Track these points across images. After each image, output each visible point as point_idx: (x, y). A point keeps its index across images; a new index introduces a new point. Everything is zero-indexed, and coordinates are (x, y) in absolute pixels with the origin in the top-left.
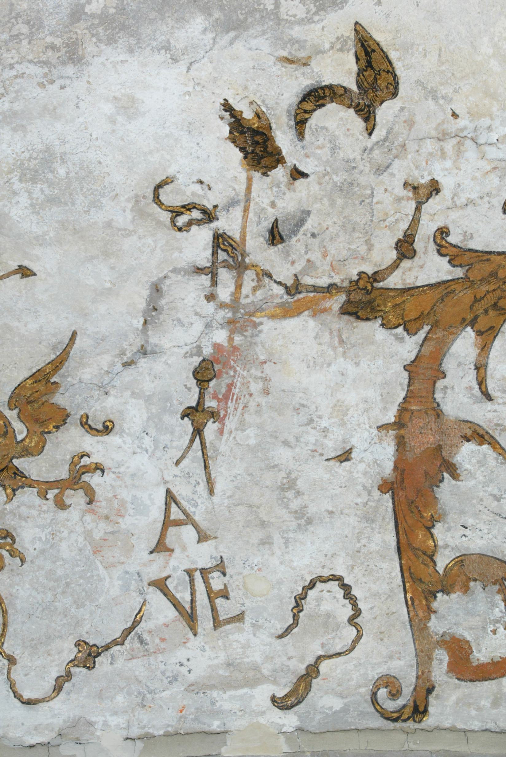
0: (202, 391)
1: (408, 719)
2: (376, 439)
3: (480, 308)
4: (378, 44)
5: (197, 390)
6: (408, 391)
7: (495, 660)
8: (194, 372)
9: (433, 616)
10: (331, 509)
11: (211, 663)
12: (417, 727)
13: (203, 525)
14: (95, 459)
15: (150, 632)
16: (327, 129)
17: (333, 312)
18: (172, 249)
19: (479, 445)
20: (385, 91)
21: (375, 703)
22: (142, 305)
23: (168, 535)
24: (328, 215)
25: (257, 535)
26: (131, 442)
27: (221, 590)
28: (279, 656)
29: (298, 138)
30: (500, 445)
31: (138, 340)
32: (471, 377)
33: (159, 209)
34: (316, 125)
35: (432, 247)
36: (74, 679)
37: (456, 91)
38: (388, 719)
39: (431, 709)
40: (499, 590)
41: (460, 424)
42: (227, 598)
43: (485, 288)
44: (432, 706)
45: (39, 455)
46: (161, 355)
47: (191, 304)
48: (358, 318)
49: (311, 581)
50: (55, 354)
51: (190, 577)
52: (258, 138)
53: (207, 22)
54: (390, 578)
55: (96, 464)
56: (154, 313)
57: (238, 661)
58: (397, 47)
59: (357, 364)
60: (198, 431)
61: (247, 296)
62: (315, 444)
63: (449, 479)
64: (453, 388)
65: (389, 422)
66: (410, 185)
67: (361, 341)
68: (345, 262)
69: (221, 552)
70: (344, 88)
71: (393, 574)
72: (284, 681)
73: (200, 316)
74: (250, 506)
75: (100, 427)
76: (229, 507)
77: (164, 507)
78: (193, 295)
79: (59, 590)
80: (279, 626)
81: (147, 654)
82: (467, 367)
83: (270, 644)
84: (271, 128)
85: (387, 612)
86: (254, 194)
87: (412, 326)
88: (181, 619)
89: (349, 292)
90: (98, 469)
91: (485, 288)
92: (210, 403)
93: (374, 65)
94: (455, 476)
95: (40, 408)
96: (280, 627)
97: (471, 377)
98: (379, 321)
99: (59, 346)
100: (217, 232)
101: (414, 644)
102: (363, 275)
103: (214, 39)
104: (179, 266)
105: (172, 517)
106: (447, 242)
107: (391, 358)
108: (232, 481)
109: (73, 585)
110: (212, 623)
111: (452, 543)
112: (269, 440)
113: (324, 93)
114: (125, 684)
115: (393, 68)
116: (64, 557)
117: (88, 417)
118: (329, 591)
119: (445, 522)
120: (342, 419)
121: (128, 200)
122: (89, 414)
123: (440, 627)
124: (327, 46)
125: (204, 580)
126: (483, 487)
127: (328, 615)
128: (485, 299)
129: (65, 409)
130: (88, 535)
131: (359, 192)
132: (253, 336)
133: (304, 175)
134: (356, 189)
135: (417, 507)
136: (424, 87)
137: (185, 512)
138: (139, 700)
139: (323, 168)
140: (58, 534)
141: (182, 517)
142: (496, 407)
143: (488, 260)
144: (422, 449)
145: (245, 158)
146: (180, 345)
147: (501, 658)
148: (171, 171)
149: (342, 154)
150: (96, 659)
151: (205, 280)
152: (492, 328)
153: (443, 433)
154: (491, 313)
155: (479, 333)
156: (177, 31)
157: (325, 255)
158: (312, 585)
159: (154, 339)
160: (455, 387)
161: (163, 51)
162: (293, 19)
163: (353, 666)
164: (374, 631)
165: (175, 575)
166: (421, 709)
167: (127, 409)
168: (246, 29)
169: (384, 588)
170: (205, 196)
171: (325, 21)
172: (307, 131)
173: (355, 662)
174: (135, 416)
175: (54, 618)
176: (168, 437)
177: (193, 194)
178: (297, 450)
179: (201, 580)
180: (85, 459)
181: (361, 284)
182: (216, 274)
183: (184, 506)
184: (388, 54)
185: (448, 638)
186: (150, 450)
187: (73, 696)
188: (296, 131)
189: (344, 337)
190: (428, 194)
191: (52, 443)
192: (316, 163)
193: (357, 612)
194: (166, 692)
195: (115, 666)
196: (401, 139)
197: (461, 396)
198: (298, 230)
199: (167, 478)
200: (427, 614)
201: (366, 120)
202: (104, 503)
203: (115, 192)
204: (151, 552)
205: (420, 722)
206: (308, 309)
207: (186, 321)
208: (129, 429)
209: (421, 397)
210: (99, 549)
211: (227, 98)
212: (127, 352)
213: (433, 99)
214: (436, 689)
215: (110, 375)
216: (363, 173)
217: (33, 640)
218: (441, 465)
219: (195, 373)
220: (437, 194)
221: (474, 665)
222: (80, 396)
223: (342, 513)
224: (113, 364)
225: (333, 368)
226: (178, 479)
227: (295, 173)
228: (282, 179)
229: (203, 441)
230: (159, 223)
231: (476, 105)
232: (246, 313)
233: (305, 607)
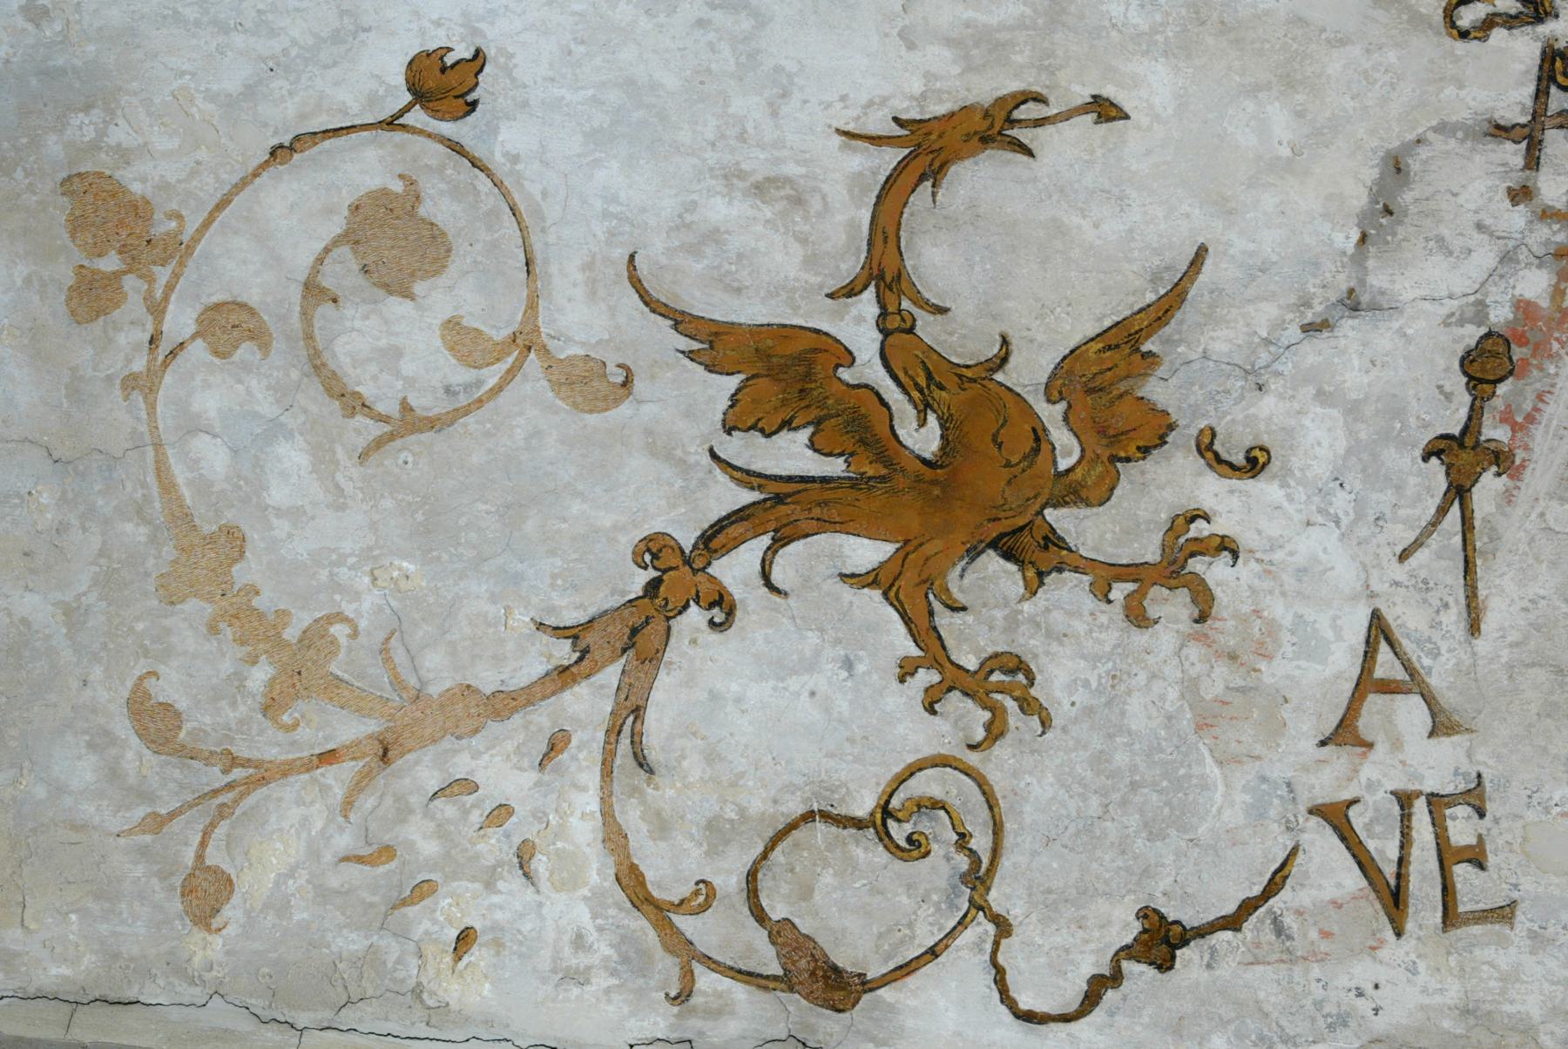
0: (1478, 403)
5: (1467, 399)
11: (1427, 1001)
13: (1448, 698)
14: (1221, 526)
15: (1299, 913)
18: (1441, 79)
22: (1358, 198)
23: (1364, 711)
26: (1304, 498)
31: (1341, 277)
42: (1481, 866)
45: (1101, 505)
46: (1391, 316)
47: (1472, 206)
50: (1157, 292)
51: (1402, 808)
55: (1223, 537)
56: (1383, 221)
57: (1487, 1007)
60: (1459, 491)
69: (1478, 763)
73: (1491, 234)
75: (1239, 459)
76: (1510, 667)
77: (1361, 648)
78: (1480, 186)
79: (1116, 796)
81: (1290, 958)
88: (1373, 896)
90: (1226, 549)
92: (1494, 432)
95: (1112, 403)
99: (1166, 276)
100: (1551, 46)
104: (1454, 119)
105: (1379, 673)
108: (1525, 610)
109: (1145, 791)
110: (1439, 914)
114: (1233, 1015)
116: (1134, 728)
117: (1214, 435)
122: (1217, 429)
125: (1433, 819)
130: (1190, 687)
140: (1125, 677)
141: (1400, 674)
146: (1436, 295)
150: (1178, 952)
151: (1513, 154)
159: (1378, 279)
165: (1369, 799)
167: (1302, 426)
174: (1319, 444)
175: (1099, 853)
176: (1388, 496)
179: (1427, 818)
180: (1200, 523)
182: (1540, 142)
183: (1408, 650)
186: (1345, 521)
187: (1121, 1021)
191: (1131, 482)
195: (1217, 973)
199: (1376, 586)
202: (1231, 623)
204: (1323, 743)
207: (1456, 244)
208: (1302, 470)
210: (1209, 721)
212: (1316, 302)
215: (1272, 349)
217: (1050, 891)
219: (1467, 361)
222: (1201, 388)
224: (1280, 325)
226: (1402, 590)
229: (1468, 514)
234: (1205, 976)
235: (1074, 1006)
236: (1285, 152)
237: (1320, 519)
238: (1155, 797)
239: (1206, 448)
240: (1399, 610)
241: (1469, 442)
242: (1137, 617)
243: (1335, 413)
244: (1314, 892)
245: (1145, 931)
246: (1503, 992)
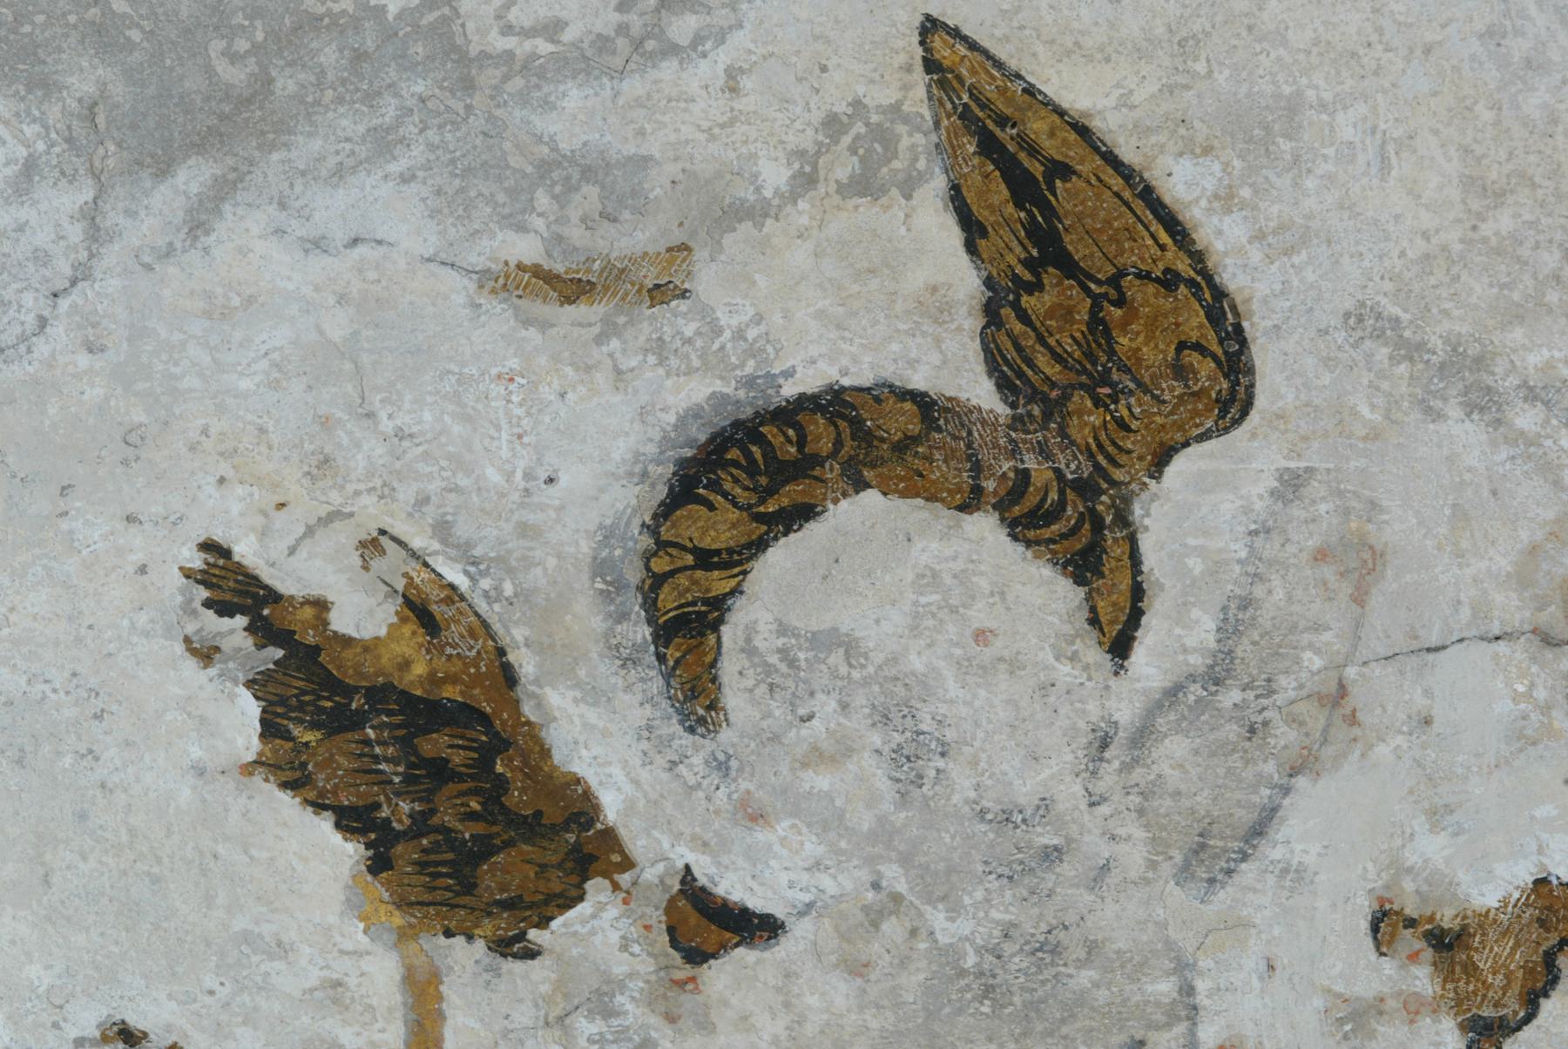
4: (1083, 131)
16: (850, 647)
20: (1171, 389)
29: (684, 717)
34: (783, 629)
52: (436, 744)
53: (30, 130)
58: (1201, 132)
66: (1411, 923)
84: (509, 676)
103: (91, 217)
113: (801, 443)
115: (1198, 257)
124: (775, 175)
131: (1102, 995)
134: (1086, 977)
136: (1401, 342)
139: (865, 875)
145: (379, 864)
149: (963, 784)
162: (544, 47)
171: (739, 39)
172: (729, 667)
184: (1155, 176)
188: (668, 677)
190: (1529, 971)
192: (812, 847)
211: (219, 536)
213: (1470, 408)
216: (1113, 879)
227: (694, 918)
228: (620, 966)
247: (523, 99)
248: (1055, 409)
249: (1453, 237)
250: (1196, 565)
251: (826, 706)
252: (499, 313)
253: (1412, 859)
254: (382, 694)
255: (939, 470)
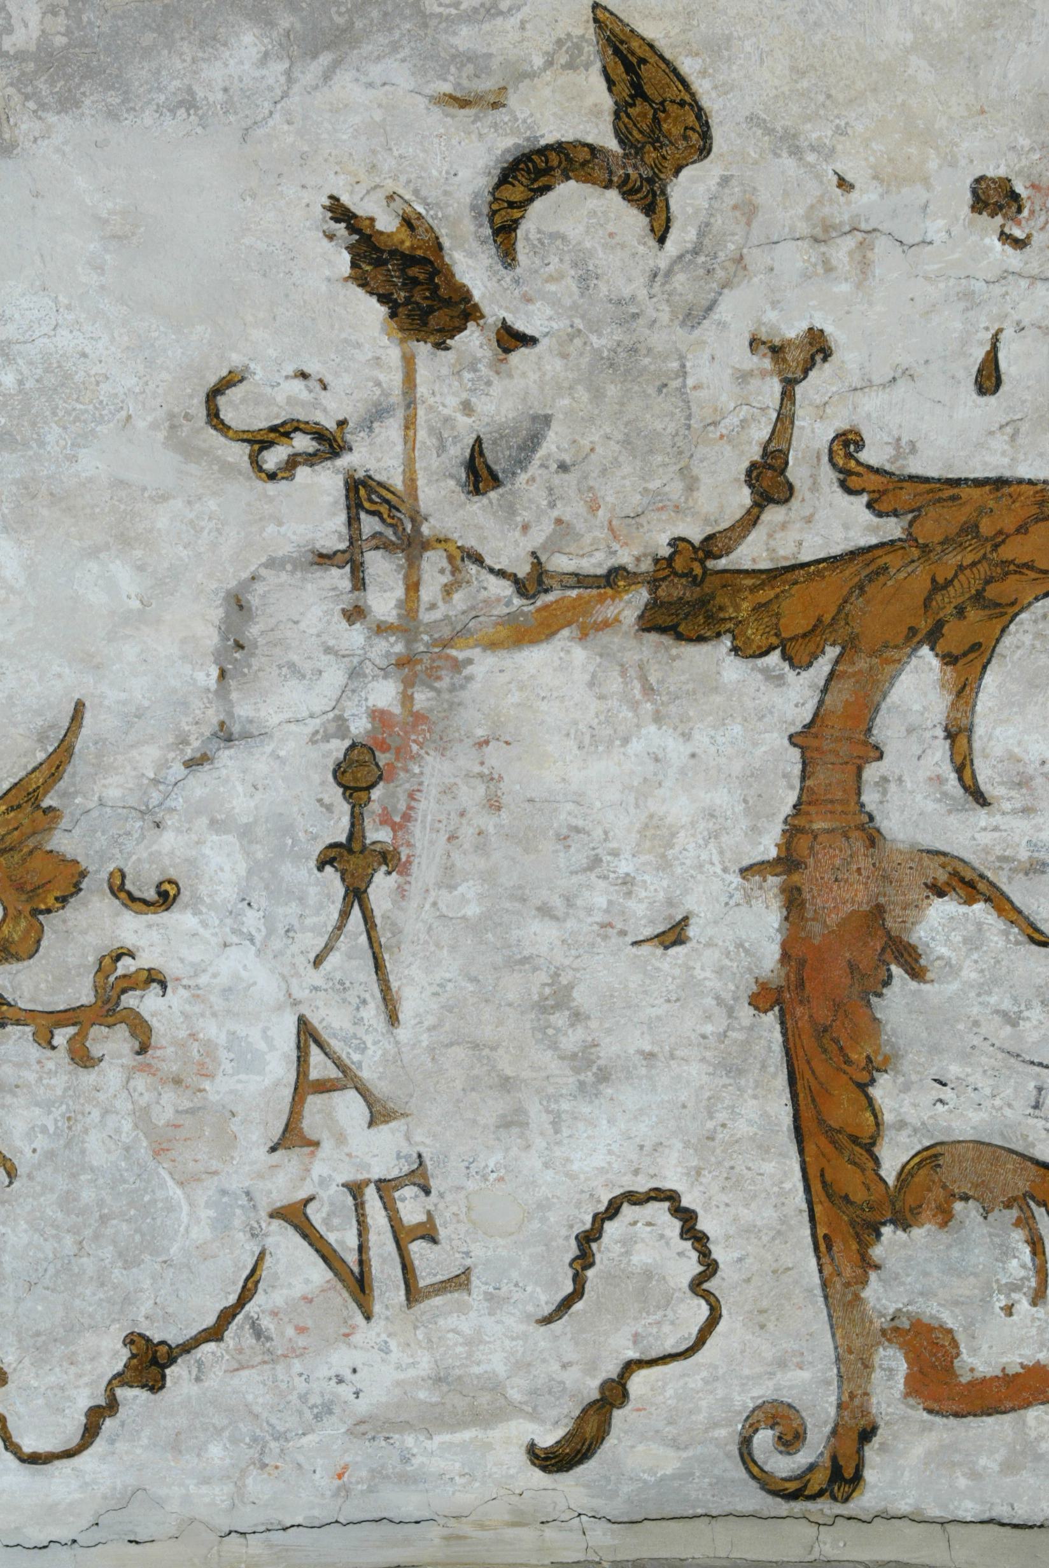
0: (357, 810)
1: (820, 1494)
2: (738, 896)
3: (946, 603)
4: (651, 46)
5: (347, 808)
6: (802, 789)
7: (1011, 1371)
8: (335, 772)
9: (873, 1276)
10: (648, 1048)
11: (402, 1376)
12: (838, 1512)
13: (381, 1087)
14: (146, 960)
15: (274, 1314)
16: (564, 238)
17: (624, 628)
18: (261, 519)
19: (965, 903)
20: (682, 144)
21: (748, 1459)
22: (211, 638)
23: (306, 1113)
24: (592, 420)
25: (493, 1107)
26: (217, 922)
27: (420, 1225)
28: (544, 1361)
29: (503, 263)
30: (1012, 903)
31: (210, 712)
32: (938, 755)
33: (222, 439)
34: (539, 231)
35: (828, 475)
36: (123, 1412)
37: (841, 132)
38: (775, 1493)
39: (869, 1475)
40: (1019, 1220)
41: (921, 859)
42: (434, 1241)
43: (953, 559)
44: (873, 1468)
45: (31, 957)
46: (262, 741)
47: (314, 631)
48: (679, 637)
49: (611, 1202)
50: (46, 750)
51: (355, 1198)
52: (414, 271)
53: (266, 41)
54: (779, 1195)
55: (149, 970)
56: (237, 655)
57: (457, 1372)
59: (687, 736)
60: (356, 894)
61: (433, 606)
62: (607, 911)
63: (902, 979)
64: (900, 780)
65: (766, 858)
66: (764, 343)
67: (690, 686)
68: (642, 520)
69: (417, 1144)
70: (589, 146)
71: (787, 1186)
72: (554, 1413)
73: (336, 654)
74: (476, 1046)
75: (151, 895)
76: (431, 1049)
77: (294, 1054)
78: (317, 611)
79: (88, 1232)
80: (543, 1298)
81: (272, 1358)
82: (928, 735)
83: (525, 1336)
84: (440, 247)
85: (775, 1266)
86: (422, 390)
87: (800, 651)
88: (339, 1285)
89: (654, 583)
90: (153, 981)
91: (953, 559)
92: (377, 834)
93: (649, 91)
94: (916, 973)
95: (24, 860)
96: (547, 1302)
97: (939, 753)
98: (727, 642)
99: (51, 734)
100: (352, 477)
101: (833, 1335)
102: (682, 545)
103: (288, 73)
104: (280, 554)
105: (314, 1075)
106: (858, 463)
107: (761, 719)
108: (436, 994)
109: (114, 1222)
110: (402, 1292)
111: (913, 1116)
112: (508, 905)
113: (547, 162)
114: (226, 1422)
116: (95, 1163)
117: (123, 876)
118: (649, 1224)
119: (897, 1072)
120: (663, 856)
121: (155, 426)
122: (126, 870)
123: (888, 1299)
124: (538, 61)
125: (384, 1204)
126: (979, 995)
127: (648, 1274)
128: (956, 582)
129: (76, 862)
130: (142, 1116)
131: (652, 367)
132: (453, 689)
133: (528, 340)
134: (647, 361)
135: (836, 1041)
136: (766, 128)
137: (339, 1064)
138: (253, 1453)
139: (568, 322)
140: (80, 1117)
141: (333, 1073)
142: (998, 819)
143: (954, 498)
144: (842, 915)
145: (393, 315)
146: (299, 716)
147: (1022, 1365)
148: (236, 359)
149: (604, 289)
150: (168, 1371)
151: (340, 578)
152: (976, 647)
153: (886, 878)
154: (972, 614)
155: (949, 659)
156: (204, 66)
157: (593, 507)
158: (613, 1210)
159: (243, 710)
160: (905, 778)
161: (182, 112)
162: (453, 11)
163: (700, 1384)
164: (746, 1308)
165: (323, 1195)
166: (848, 1473)
167: (204, 856)
168: (355, 43)
169: (769, 1215)
170: (316, 404)
171: (526, 10)
172: (520, 245)
173: (704, 1374)
174: (222, 870)
175: (79, 1289)
176: (293, 908)
177: (291, 401)
178: (570, 924)
179: (379, 1204)
180: (126, 961)
181: (679, 564)
182: (362, 564)
183: (337, 1049)
184: (677, 64)
185: (905, 1324)
186: (259, 938)
187: (121, 1446)
188: (498, 248)
189: (652, 680)
190: (805, 361)
191: (55, 932)
192: (549, 312)
193: (710, 1268)
194: (310, 1437)
195: (206, 1384)
196: (731, 247)
197: (919, 797)
198: (529, 459)
199: (297, 994)
200: (860, 1271)
201: (649, 210)
202: (170, 1050)
203: (124, 414)
204: (273, 1149)
205: (846, 1500)
206: (569, 624)
207: (307, 667)
208: (210, 896)
209: (832, 802)
210: (164, 1146)
211: (335, 193)
212: (192, 738)
213: (791, 154)
214: (880, 1432)
215: (161, 787)
216: (657, 325)
217: (38, 1334)
218: (883, 950)
219: (339, 773)
220: (825, 360)
221: (964, 1380)
222: (103, 833)
223: (672, 1057)
224: (164, 764)
225: (635, 746)
226: (322, 994)
227: (506, 337)
228: (480, 353)
229: (368, 914)
230: (228, 469)
231: (890, 160)
232: (435, 642)
233: (598, 1258)
234: (195, 1389)
235: (75, 1441)
236: (135, 604)
237: (235, 939)
238: (124, 1226)
239: (119, 888)
240: (322, 1012)
241: (356, 847)
242: (83, 1058)
243: (229, 838)
244: (285, 1291)
245: (133, 1356)
246: (470, 1355)
247: (446, 31)
248: (639, 151)
249: (786, 89)
250: (690, 210)
251: (555, 260)
252: (437, 112)
253: (765, 320)
254: (394, 253)
255: (596, 173)
